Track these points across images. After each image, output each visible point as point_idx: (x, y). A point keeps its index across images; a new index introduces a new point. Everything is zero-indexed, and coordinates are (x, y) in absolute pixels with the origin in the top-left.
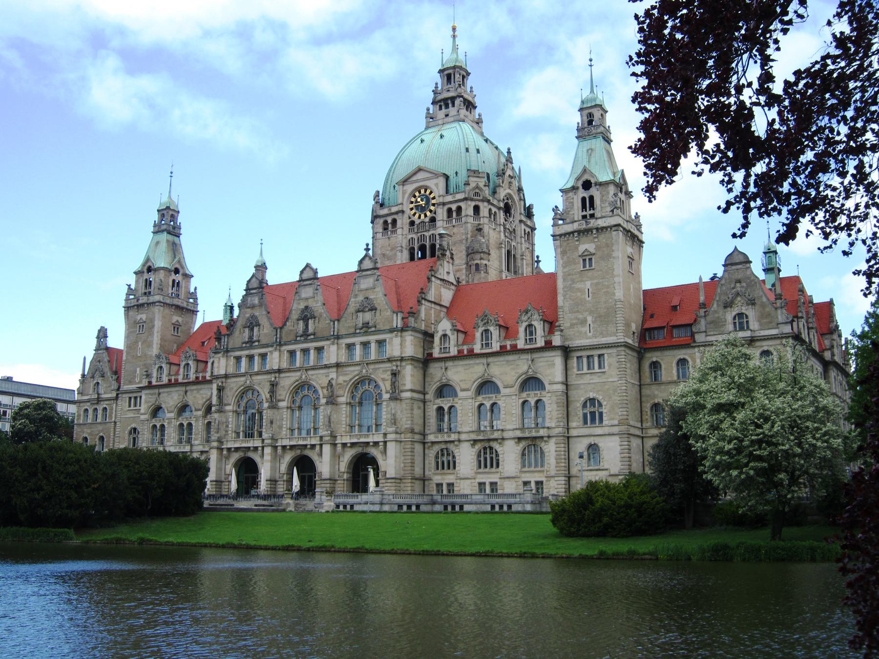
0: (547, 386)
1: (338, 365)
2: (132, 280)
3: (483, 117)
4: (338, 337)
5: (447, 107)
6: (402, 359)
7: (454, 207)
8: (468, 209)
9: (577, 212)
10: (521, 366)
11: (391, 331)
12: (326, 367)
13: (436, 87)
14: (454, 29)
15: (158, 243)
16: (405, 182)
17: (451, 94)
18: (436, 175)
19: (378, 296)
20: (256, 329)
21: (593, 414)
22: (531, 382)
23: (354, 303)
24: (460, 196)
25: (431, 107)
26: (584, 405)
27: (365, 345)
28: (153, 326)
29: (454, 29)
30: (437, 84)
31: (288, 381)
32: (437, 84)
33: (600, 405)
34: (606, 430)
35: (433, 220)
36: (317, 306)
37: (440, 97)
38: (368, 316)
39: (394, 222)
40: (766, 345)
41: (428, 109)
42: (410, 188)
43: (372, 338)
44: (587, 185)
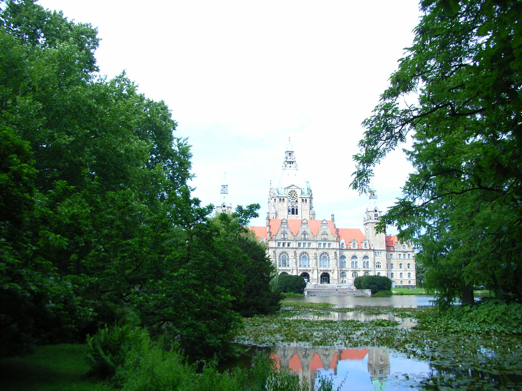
0: (370, 258)
1: (317, 249)
4: (317, 241)
5: (290, 163)
6: (337, 249)
7: (304, 199)
8: (308, 200)
9: (374, 218)
10: (364, 253)
11: (333, 241)
12: (313, 249)
16: (288, 188)
17: (292, 160)
18: (299, 188)
19: (328, 231)
22: (366, 257)
23: (321, 232)
24: (308, 197)
27: (324, 244)
31: (299, 252)
35: (297, 201)
36: (308, 231)
37: (287, 160)
38: (325, 236)
39: (283, 199)
40: (409, 253)
42: (289, 190)
43: (327, 243)
44: (376, 211)
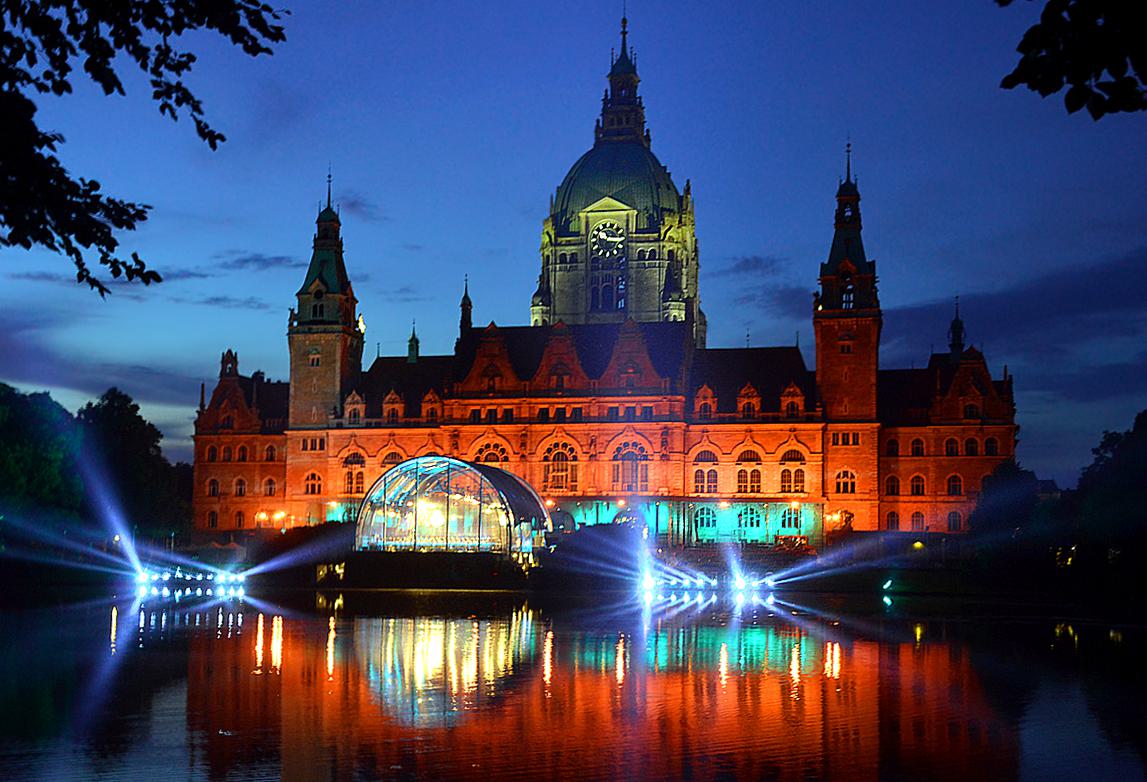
2: (295, 303)
3: (651, 133)
13: (606, 95)
14: (624, 21)
15: (323, 263)
20: (497, 379)
21: (846, 484)
25: (600, 118)
26: (839, 476)
28: (334, 361)
29: (624, 21)
30: (606, 91)
32: (606, 91)
33: (853, 476)
34: (859, 496)
41: (598, 121)
